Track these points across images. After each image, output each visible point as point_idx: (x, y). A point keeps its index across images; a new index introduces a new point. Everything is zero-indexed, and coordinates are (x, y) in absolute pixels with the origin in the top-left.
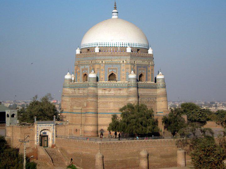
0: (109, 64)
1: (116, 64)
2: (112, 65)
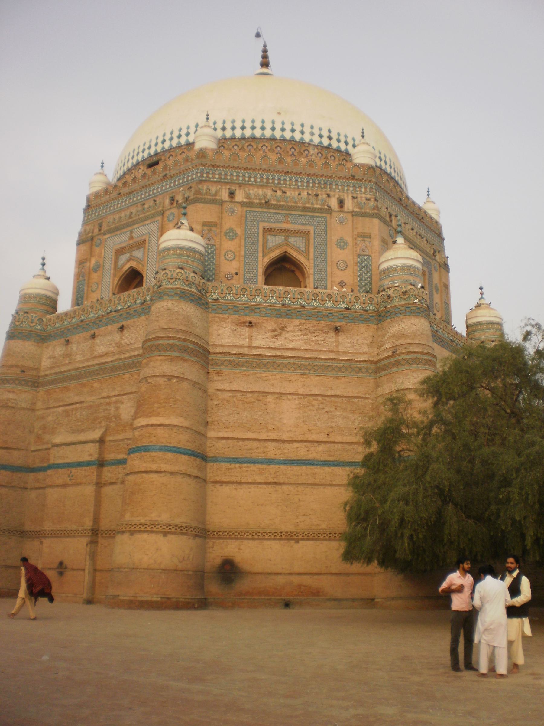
1: (305, 209)
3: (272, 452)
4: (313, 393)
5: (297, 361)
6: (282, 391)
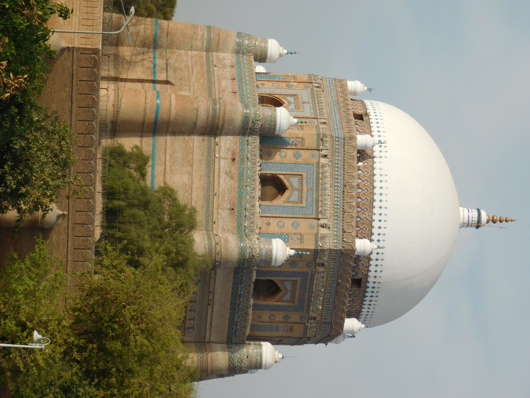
0: (318, 178)
1: (317, 201)
2: (312, 190)
4: (193, 193)
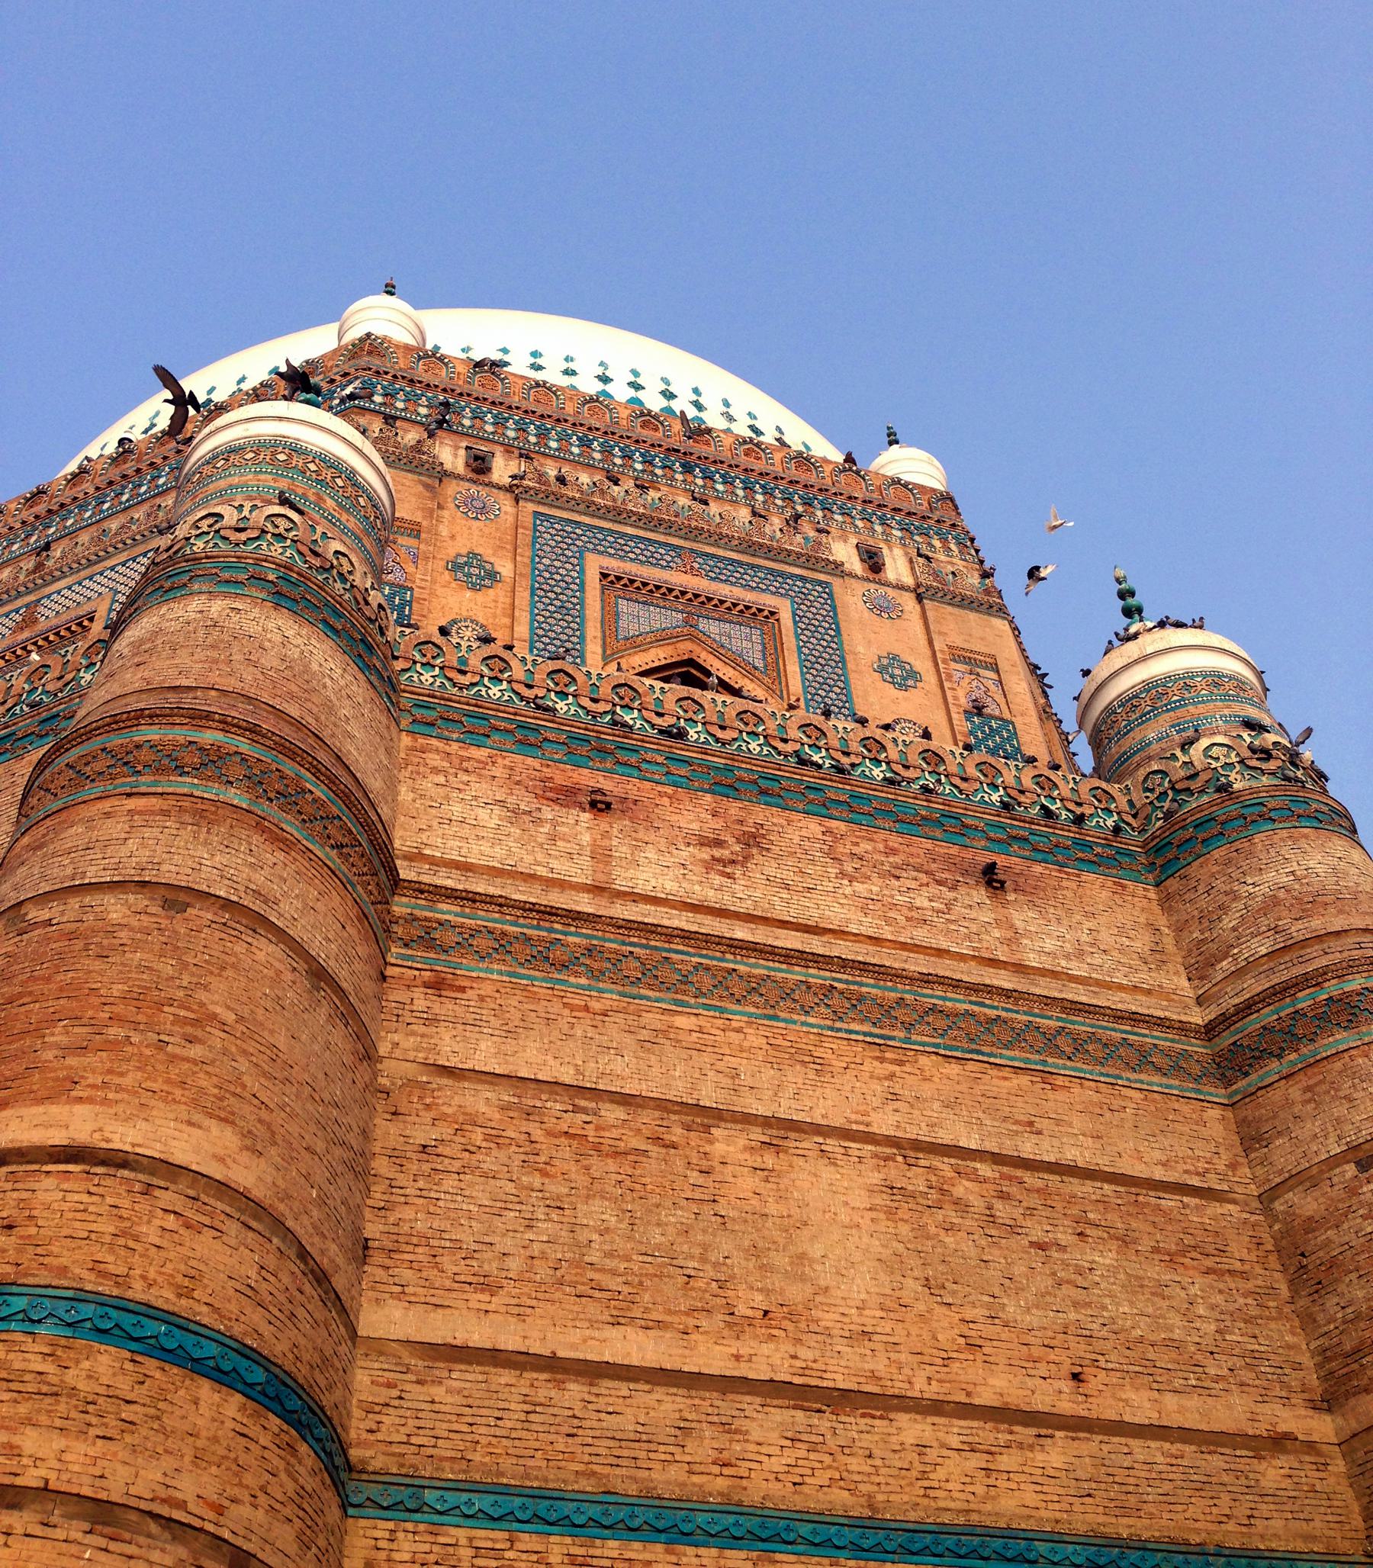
3: (776, 1464)
4: (944, 1137)
5: (841, 980)
6: (785, 1110)
